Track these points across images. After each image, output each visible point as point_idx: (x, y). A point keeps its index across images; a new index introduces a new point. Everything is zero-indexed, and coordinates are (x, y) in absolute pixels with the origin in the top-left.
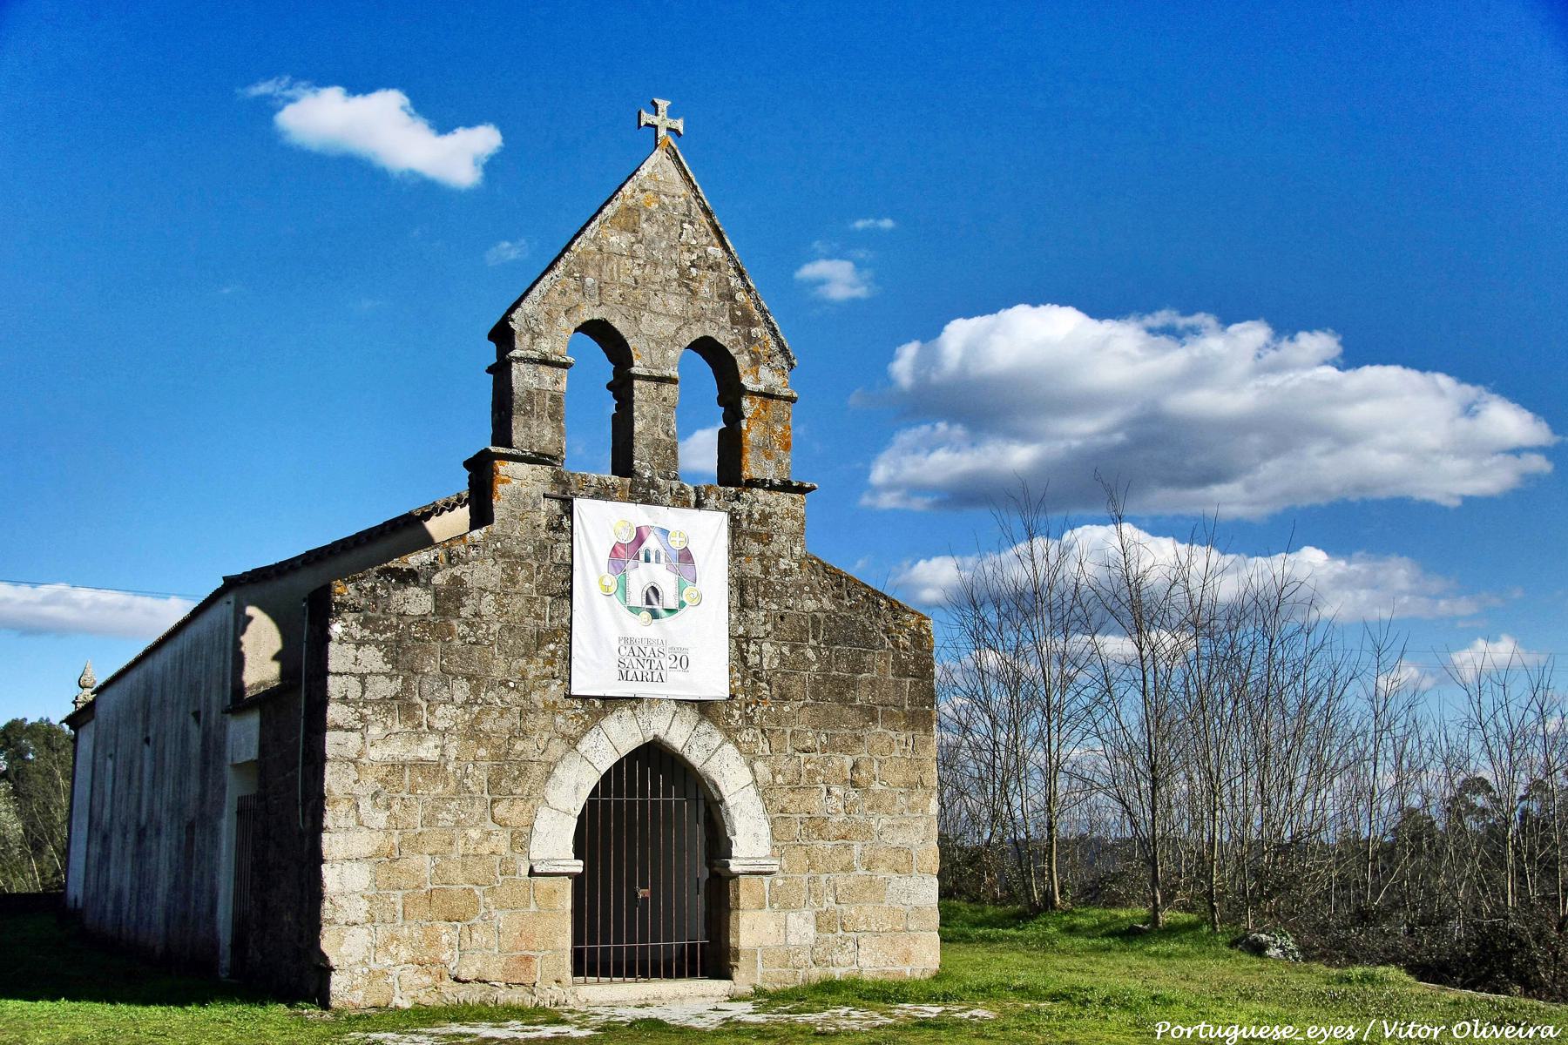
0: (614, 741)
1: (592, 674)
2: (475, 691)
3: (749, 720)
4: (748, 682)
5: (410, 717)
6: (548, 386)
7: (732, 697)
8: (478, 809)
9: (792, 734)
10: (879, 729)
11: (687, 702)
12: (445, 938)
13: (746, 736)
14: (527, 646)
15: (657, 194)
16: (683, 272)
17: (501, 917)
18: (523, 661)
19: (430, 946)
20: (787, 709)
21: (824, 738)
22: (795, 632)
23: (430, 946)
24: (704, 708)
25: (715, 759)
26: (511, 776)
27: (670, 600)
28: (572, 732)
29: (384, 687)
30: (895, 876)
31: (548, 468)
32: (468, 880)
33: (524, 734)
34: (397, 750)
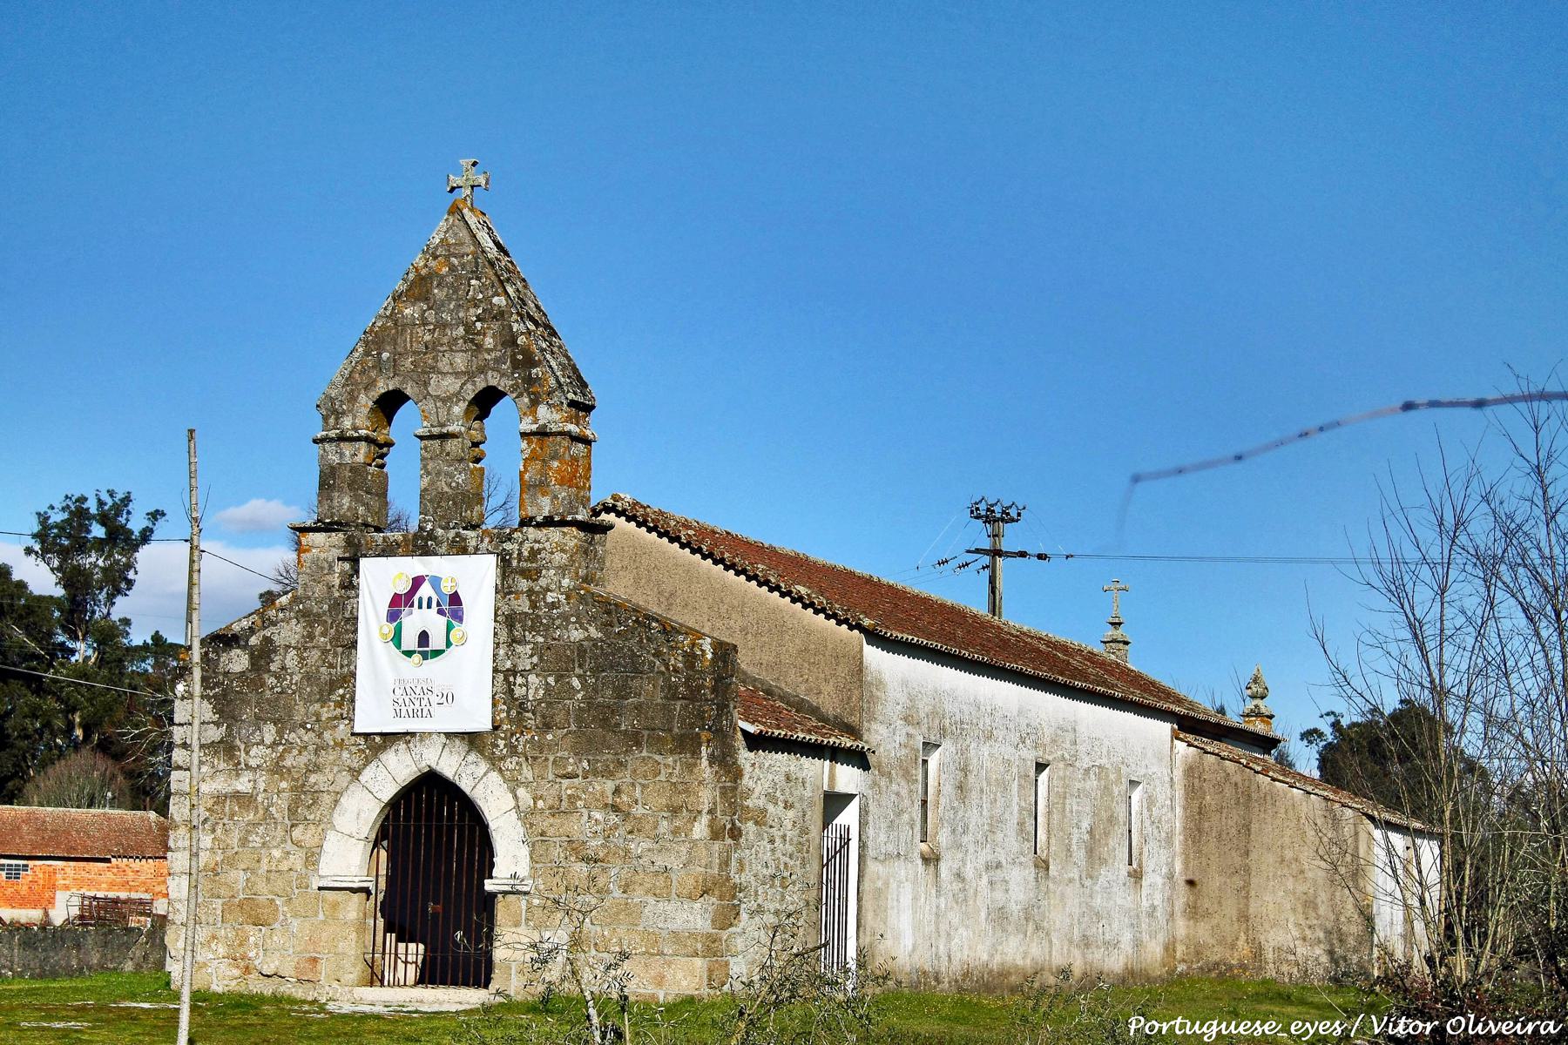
0: (392, 774)
1: (371, 714)
2: (280, 733)
3: (513, 750)
4: (513, 713)
5: (232, 757)
6: (347, 460)
7: (496, 728)
8: (280, 832)
9: (554, 762)
10: (644, 754)
11: (456, 734)
12: (252, 939)
13: (510, 764)
14: (321, 692)
15: (447, 257)
16: (469, 328)
17: (295, 924)
18: (317, 706)
19: (241, 945)
20: (550, 737)
21: (585, 764)
22: (557, 661)
23: (241, 945)
24: (472, 740)
25: (480, 786)
26: (307, 803)
27: (436, 642)
28: (355, 765)
29: (215, 734)
30: (651, 900)
31: (341, 535)
32: (271, 892)
33: (317, 768)
34: (219, 785)
